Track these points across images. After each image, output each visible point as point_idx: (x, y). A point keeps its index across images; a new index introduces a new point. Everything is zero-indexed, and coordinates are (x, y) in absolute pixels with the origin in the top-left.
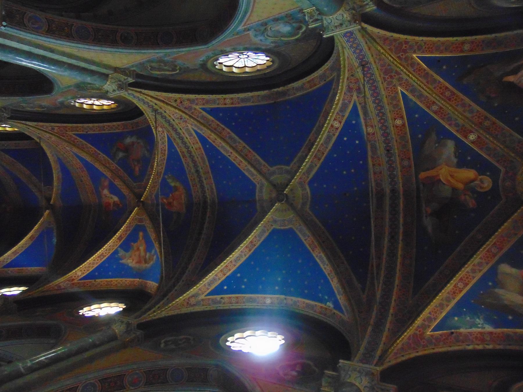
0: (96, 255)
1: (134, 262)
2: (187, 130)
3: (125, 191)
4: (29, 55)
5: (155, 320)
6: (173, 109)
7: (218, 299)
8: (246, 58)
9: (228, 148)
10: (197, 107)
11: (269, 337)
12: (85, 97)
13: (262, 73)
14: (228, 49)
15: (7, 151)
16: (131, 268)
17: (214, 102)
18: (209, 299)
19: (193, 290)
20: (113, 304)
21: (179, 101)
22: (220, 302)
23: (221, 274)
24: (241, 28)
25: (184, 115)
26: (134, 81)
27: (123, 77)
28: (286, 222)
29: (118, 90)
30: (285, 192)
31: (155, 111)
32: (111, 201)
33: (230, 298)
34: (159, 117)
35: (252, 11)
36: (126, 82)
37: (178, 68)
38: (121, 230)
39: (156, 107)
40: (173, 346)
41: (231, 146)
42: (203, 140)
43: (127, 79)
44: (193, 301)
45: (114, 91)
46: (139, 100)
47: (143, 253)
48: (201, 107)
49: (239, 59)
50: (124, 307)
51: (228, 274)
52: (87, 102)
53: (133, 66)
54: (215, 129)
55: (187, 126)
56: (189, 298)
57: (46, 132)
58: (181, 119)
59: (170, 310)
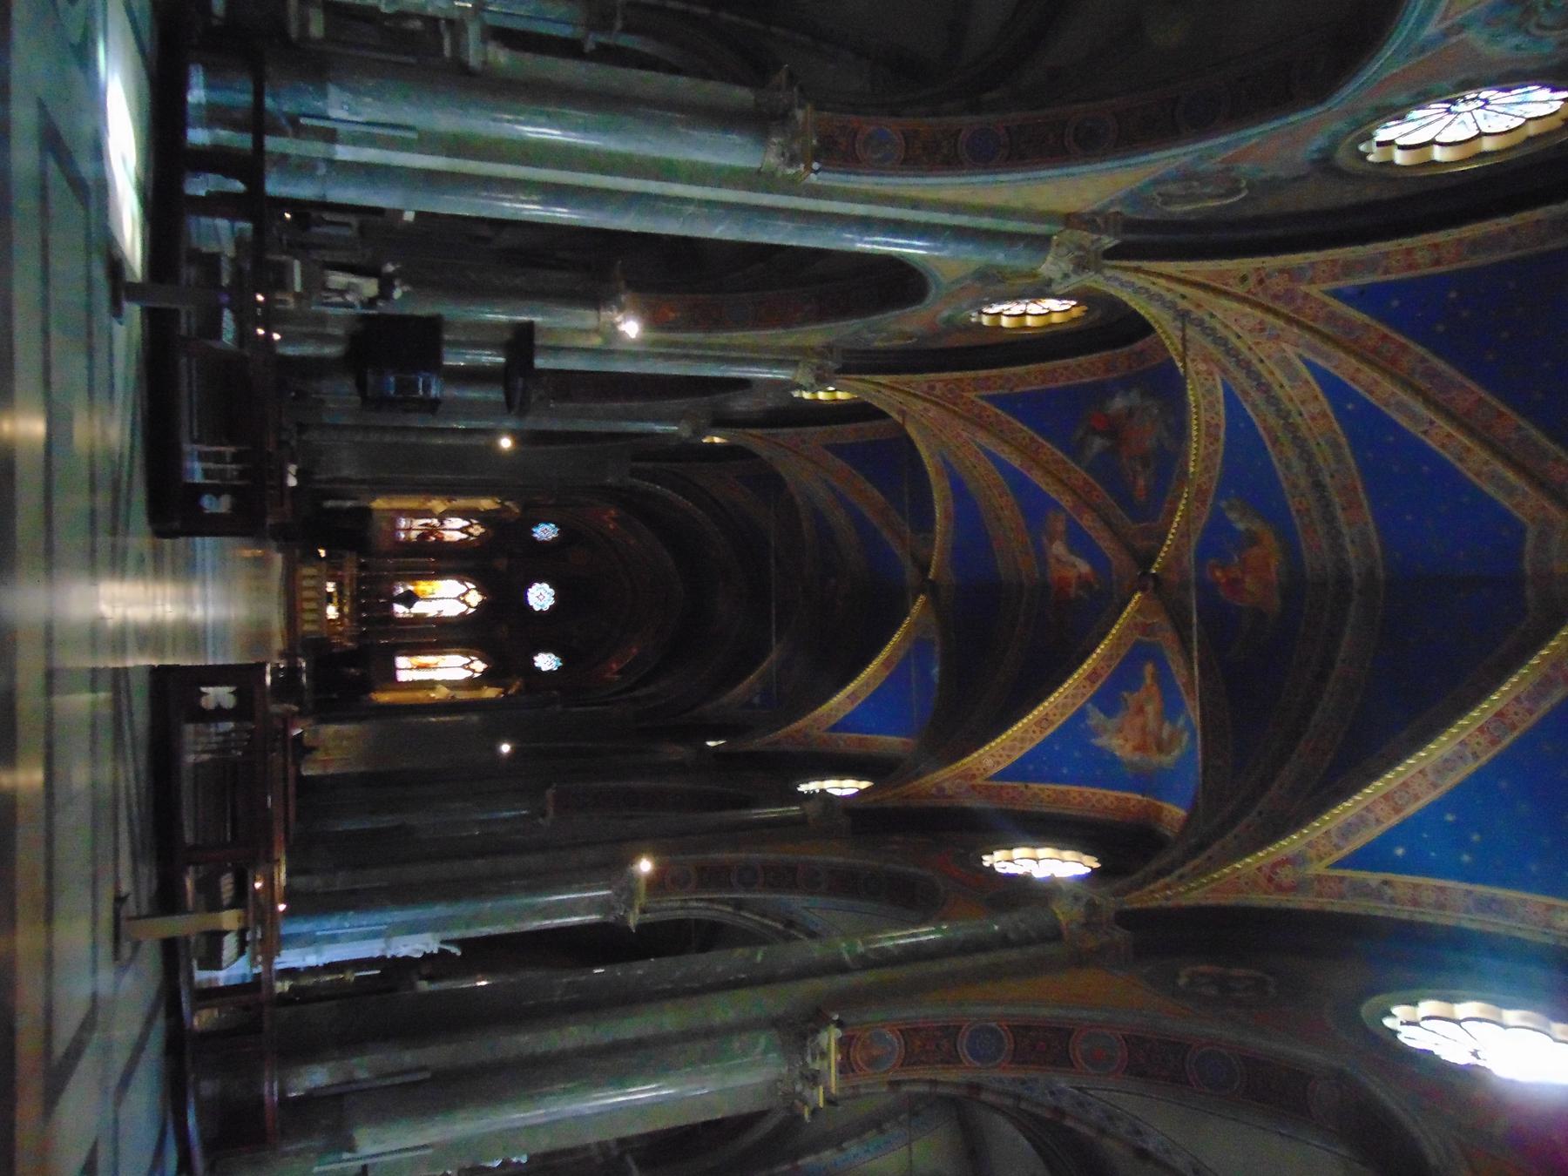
0: (1030, 717)
1: (1129, 747)
2: (1285, 363)
3: (1106, 544)
4: (866, 225)
6: (1235, 305)
8: (1482, 107)
9: (1419, 407)
10: (1314, 290)
11: (1556, 1040)
12: (1001, 299)
13: (1541, 145)
14: (1402, 98)
16: (1115, 761)
17: (1370, 265)
18: (1342, 879)
19: (1291, 844)
20: (1068, 854)
21: (1252, 281)
24: (1431, 30)
25: (1270, 319)
26: (1117, 242)
27: (1085, 237)
29: (1075, 271)
31: (1183, 316)
32: (1071, 574)
33: (1416, 886)
34: (1192, 332)
36: (1097, 248)
37: (1244, 183)
38: (1094, 656)
39: (1183, 304)
40: (1213, 991)
41: (1428, 401)
42: (1334, 388)
43: (1099, 239)
44: (1286, 875)
45: (1066, 276)
47: (1152, 725)
48: (1325, 287)
49: (1453, 116)
50: (1097, 865)
52: (1009, 309)
53: (1112, 203)
54: (1375, 351)
56: (1275, 865)
57: (915, 396)
58: (1262, 330)
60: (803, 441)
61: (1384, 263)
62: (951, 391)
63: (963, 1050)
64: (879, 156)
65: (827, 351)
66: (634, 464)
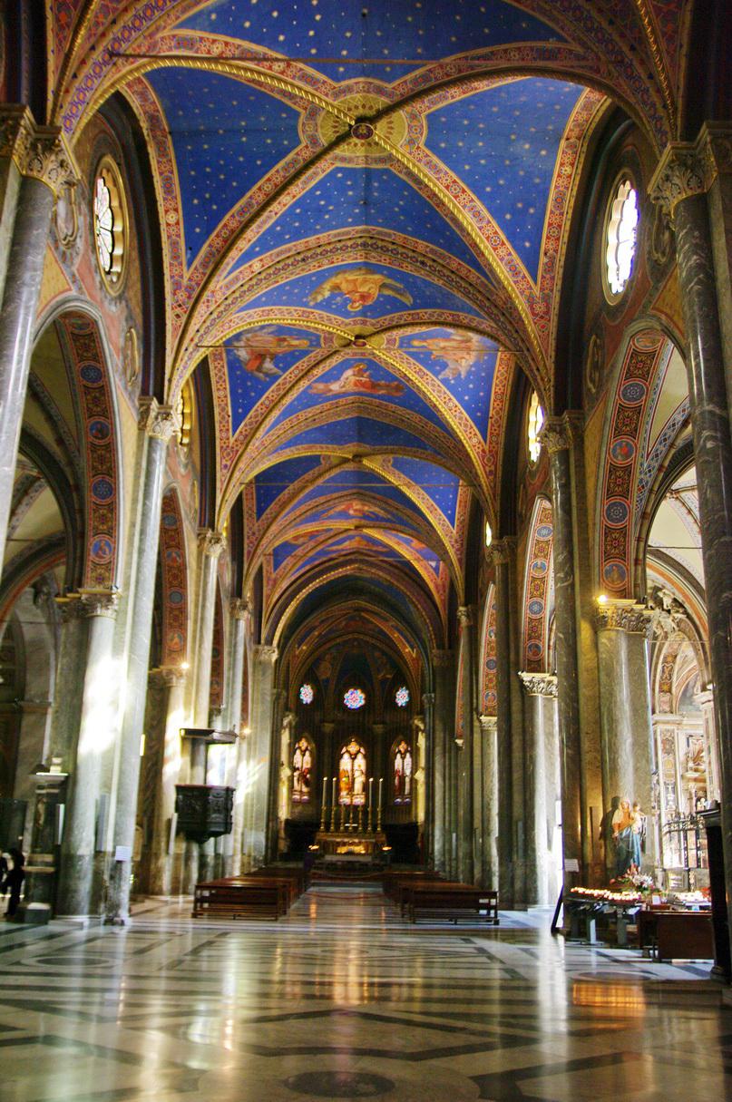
1: (467, 357)
2: (227, 287)
5: (555, 381)
7: (546, 260)
10: (187, 275)
15: (260, 512)
18: (543, 277)
21: (178, 311)
22: (552, 259)
23: (500, 251)
28: (415, 123)
30: (353, 123)
32: (353, 379)
35: (54, 298)
44: (540, 308)
46: (181, 377)
48: (185, 268)
51: (503, 237)
55: (221, 288)
56: (534, 314)
57: (231, 476)
59: (546, 351)
60: (254, 534)
61: (174, 237)
62: (229, 454)
63: (619, 525)
64: (107, 550)
65: (201, 538)
66: (263, 641)
